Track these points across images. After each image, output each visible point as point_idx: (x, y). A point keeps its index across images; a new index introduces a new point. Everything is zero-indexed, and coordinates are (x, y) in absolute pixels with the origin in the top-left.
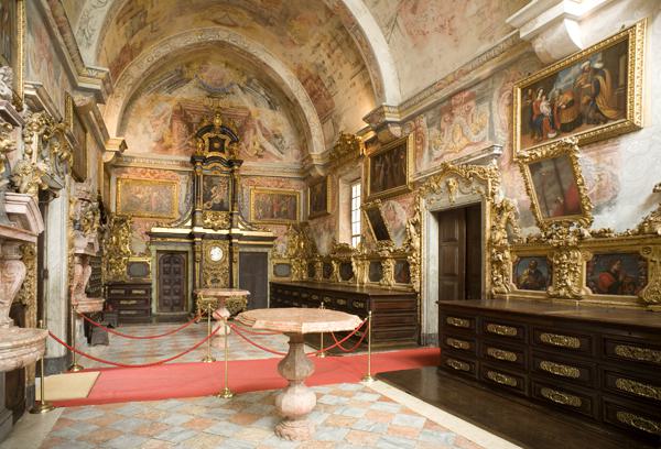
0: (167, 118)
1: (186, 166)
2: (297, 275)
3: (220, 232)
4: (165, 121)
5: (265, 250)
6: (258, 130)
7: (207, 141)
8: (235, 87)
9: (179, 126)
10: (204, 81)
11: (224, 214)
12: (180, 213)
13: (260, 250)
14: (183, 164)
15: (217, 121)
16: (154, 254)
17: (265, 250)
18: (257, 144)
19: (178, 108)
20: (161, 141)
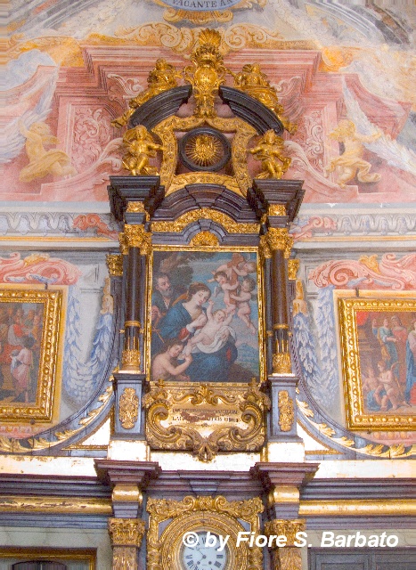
0: (41, 93)
1: (99, 232)
3: (222, 463)
4: (36, 101)
6: (352, 104)
12: (69, 399)
14: (87, 225)
15: (206, 81)
19: (80, 64)
20: (23, 160)
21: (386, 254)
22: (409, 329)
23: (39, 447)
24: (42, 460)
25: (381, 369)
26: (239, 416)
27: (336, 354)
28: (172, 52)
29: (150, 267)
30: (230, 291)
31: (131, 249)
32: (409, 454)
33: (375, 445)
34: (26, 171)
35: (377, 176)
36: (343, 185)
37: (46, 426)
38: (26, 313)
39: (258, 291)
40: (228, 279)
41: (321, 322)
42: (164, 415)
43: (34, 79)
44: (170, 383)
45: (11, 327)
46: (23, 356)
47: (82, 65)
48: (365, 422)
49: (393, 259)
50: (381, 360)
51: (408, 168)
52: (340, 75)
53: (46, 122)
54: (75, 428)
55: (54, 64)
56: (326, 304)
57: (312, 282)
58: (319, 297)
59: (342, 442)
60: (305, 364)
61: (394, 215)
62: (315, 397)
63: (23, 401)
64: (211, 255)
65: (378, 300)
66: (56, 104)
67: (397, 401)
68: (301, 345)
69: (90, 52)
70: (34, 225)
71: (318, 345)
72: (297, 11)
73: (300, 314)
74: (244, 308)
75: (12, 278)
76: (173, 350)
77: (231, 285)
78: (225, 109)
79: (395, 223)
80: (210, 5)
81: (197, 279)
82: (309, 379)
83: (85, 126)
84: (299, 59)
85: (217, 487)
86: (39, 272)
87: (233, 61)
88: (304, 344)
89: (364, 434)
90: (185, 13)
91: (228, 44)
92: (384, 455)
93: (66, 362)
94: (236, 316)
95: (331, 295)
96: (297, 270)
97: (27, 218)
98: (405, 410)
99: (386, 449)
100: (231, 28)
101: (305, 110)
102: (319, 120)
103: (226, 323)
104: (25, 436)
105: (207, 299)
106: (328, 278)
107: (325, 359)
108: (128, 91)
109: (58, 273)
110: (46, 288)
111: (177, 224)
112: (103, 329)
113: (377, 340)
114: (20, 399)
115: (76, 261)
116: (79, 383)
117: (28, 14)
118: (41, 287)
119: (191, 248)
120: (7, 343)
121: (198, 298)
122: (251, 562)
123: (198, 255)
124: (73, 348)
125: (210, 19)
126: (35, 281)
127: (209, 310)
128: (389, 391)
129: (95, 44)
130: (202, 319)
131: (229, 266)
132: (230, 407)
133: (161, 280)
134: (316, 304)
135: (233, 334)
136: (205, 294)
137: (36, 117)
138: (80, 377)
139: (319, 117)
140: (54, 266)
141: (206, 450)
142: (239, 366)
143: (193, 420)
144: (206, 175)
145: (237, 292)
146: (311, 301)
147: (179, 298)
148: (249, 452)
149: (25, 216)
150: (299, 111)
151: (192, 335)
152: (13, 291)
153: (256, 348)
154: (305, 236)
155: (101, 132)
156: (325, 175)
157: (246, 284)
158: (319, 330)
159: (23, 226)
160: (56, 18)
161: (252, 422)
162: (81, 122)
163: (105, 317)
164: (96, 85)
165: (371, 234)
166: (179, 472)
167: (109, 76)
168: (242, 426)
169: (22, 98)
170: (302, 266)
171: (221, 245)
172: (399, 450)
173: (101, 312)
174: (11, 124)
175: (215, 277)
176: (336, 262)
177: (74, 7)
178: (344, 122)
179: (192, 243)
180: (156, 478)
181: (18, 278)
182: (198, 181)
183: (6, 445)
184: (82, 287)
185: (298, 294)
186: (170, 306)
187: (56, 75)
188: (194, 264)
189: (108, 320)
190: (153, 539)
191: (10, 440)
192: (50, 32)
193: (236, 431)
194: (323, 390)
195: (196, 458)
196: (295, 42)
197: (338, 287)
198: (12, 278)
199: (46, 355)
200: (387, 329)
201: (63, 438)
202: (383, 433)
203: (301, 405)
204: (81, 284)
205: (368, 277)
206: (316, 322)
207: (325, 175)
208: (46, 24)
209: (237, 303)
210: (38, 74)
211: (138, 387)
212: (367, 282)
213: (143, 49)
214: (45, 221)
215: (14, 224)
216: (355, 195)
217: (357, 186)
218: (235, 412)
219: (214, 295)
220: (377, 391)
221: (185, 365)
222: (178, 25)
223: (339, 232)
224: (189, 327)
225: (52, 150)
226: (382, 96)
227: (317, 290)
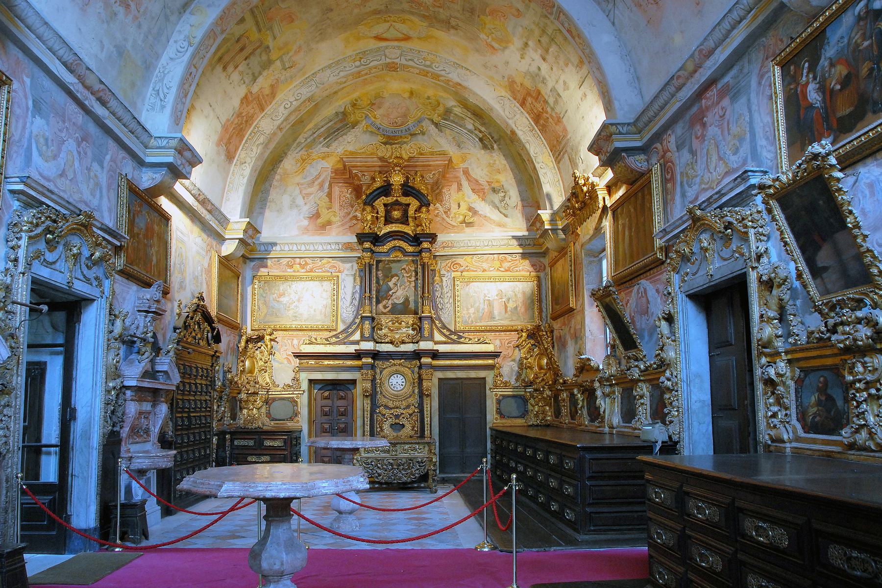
0: (323, 182)
1: (352, 250)
2: (537, 416)
3: (404, 348)
4: (321, 186)
5: (482, 374)
6: (465, 183)
7: (382, 209)
8: (426, 124)
9: (341, 192)
10: (378, 122)
11: (410, 319)
12: (344, 322)
13: (473, 374)
14: (348, 247)
15: (397, 179)
16: (305, 385)
17: (482, 374)
18: (464, 206)
19: (340, 166)
20: (317, 215)
34: (319, 221)
37: (335, 333)
43: (319, 175)
51: (488, 215)
64: (399, 261)
69: (344, 159)
70: (325, 248)
72: (441, 134)
76: (384, 302)
81: (393, 272)
90: (389, 137)
92: (470, 342)
99: (470, 339)
105: (398, 280)
109: (335, 267)
115: (343, 262)
117: (314, 139)
118: (330, 274)
121: (394, 280)
123: (394, 261)
134: (444, 279)
145: (410, 277)
149: (321, 244)
158: (445, 290)
159: (320, 248)
162: (342, 195)
166: (387, 352)
178: (460, 193)
185: (437, 275)
188: (392, 265)
189: (358, 288)
190: (378, 377)
192: (325, 149)
194: (446, 316)
204: (346, 272)
215: (316, 248)
221: (389, 308)
222: (385, 144)
224: (390, 293)
225: (330, 210)
226: (479, 178)
227: (445, 273)
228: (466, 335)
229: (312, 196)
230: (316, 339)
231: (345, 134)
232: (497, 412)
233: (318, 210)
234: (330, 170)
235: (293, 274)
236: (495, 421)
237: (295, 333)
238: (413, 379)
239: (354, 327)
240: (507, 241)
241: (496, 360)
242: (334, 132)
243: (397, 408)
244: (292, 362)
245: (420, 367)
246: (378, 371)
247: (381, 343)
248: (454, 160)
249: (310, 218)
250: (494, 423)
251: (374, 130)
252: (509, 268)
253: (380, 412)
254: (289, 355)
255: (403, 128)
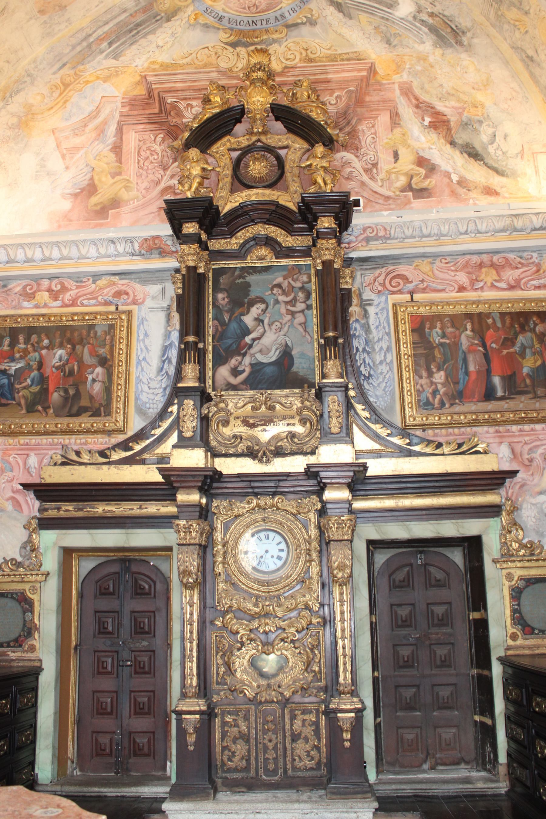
0: (105, 122)
1: (163, 253)
4: (101, 131)
12: (141, 411)
19: (141, 91)
21: (439, 259)
22: (461, 330)
23: (115, 456)
24: (119, 469)
25: (434, 370)
26: (296, 421)
27: (392, 357)
28: (228, 73)
29: (211, 283)
30: (286, 303)
31: (188, 268)
32: (461, 450)
33: (429, 442)
34: (94, 200)
35: (430, 182)
36: (398, 193)
37: (121, 438)
38: (99, 334)
39: (314, 300)
40: (284, 291)
41: (377, 327)
42: (226, 423)
43: (98, 110)
44: (232, 393)
45: (86, 348)
46: (98, 374)
47: (144, 93)
48: (418, 421)
49: (447, 263)
50: (434, 360)
52: (394, 83)
53: (111, 150)
54: (148, 438)
55: (117, 94)
56: (382, 309)
57: (367, 289)
58: (375, 303)
59: (397, 440)
60: (362, 368)
61: (446, 219)
62: (372, 400)
63: (100, 415)
64: (267, 269)
65: (432, 304)
66: (120, 131)
67: (450, 399)
68: (357, 349)
69: (150, 79)
70: (103, 251)
71: (374, 350)
72: (350, 22)
73: (357, 321)
74: (300, 318)
75: (85, 302)
76: (233, 362)
77: (287, 297)
78: (279, 126)
79: (447, 227)
80: (264, 23)
81: (254, 292)
82: (365, 382)
83: (148, 152)
84: (353, 71)
85: (277, 487)
86: (110, 294)
87: (288, 76)
88: (361, 350)
89: (419, 433)
90: (241, 32)
91: (284, 61)
92: (438, 451)
93: (138, 378)
94: (292, 325)
95: (387, 298)
96: (353, 277)
97: (95, 244)
98: (457, 408)
99: (439, 445)
100: (285, 44)
101: (359, 121)
102: (373, 131)
103: (282, 333)
104: (103, 447)
105: (264, 311)
106: (384, 285)
107: (381, 363)
108: (186, 114)
109: (127, 294)
110: (117, 309)
111: (233, 240)
112: (171, 345)
113: (430, 342)
114: (96, 414)
116: (151, 396)
117: (89, 46)
119: (249, 262)
120: (83, 362)
121: (255, 311)
122: (310, 555)
123: (255, 270)
124: (143, 364)
125: (265, 37)
126: (107, 303)
127: (266, 322)
128: (442, 390)
129: (154, 70)
130: (260, 329)
131: (285, 278)
132: (287, 412)
133: (220, 296)
134: (371, 310)
135: (289, 344)
136: (263, 306)
137: (101, 147)
138: (151, 391)
139: (373, 126)
140: (124, 288)
141: (264, 453)
142: (296, 373)
143: (253, 426)
144: (260, 191)
145: (293, 302)
146: (368, 308)
147: (237, 312)
148: (306, 454)
149: (94, 243)
150: (354, 122)
151: (251, 346)
152: (86, 314)
153: (310, 354)
154: (360, 245)
155: (163, 157)
156: (380, 184)
157: (301, 295)
158: (375, 334)
159: (93, 252)
160: (117, 48)
161: (308, 425)
162: (144, 148)
163: (173, 333)
164: (157, 110)
165: (424, 239)
166: (239, 475)
167: (169, 101)
168: (299, 429)
169: (87, 129)
170: (358, 274)
171: (276, 258)
172: (454, 446)
173: (169, 328)
174: (80, 155)
175: (272, 289)
176: (392, 268)
177: (133, 36)
178: (397, 131)
179: (249, 258)
180: (219, 481)
181: (91, 301)
182: (253, 198)
183: (85, 456)
184: (151, 306)
185: (355, 301)
186: (230, 320)
187: (120, 106)
189: (175, 336)
190: (218, 536)
191: (90, 452)
192: (111, 62)
193: (292, 435)
194: (379, 393)
195: (257, 461)
196: (348, 53)
197: (393, 293)
198: (85, 302)
199: (119, 372)
200: (440, 332)
201: (138, 448)
202: (437, 431)
203: (359, 407)
204: (149, 303)
205: (422, 281)
206: (372, 327)
207: (380, 184)
208: (107, 56)
209: (293, 314)
210: (102, 105)
211: (198, 398)
212: (421, 286)
213: (200, 73)
214: (112, 246)
215: (84, 252)
216: (409, 202)
217: (410, 194)
218: (292, 417)
219: (270, 307)
220: (430, 390)
222: (234, 45)
223: (393, 239)
224: (248, 339)
225: (118, 178)
227: (373, 296)
228: (430, 434)
229: (82, 152)
230: (78, 453)
231: (153, 32)
232: (513, 619)
233: (92, 179)
234: (119, 100)
235: (34, 311)
236: (511, 642)
237: (34, 440)
238: (309, 542)
239: (165, 425)
240: (508, 221)
241: (503, 491)
242: (131, 31)
243: (267, 615)
244: (24, 506)
245: (322, 512)
246: (219, 526)
247: (227, 455)
248: (381, 70)
249: (76, 195)
250: (508, 648)
251: (210, 20)
252: (518, 281)
253: (224, 626)
254: (18, 491)
255: (271, 14)
